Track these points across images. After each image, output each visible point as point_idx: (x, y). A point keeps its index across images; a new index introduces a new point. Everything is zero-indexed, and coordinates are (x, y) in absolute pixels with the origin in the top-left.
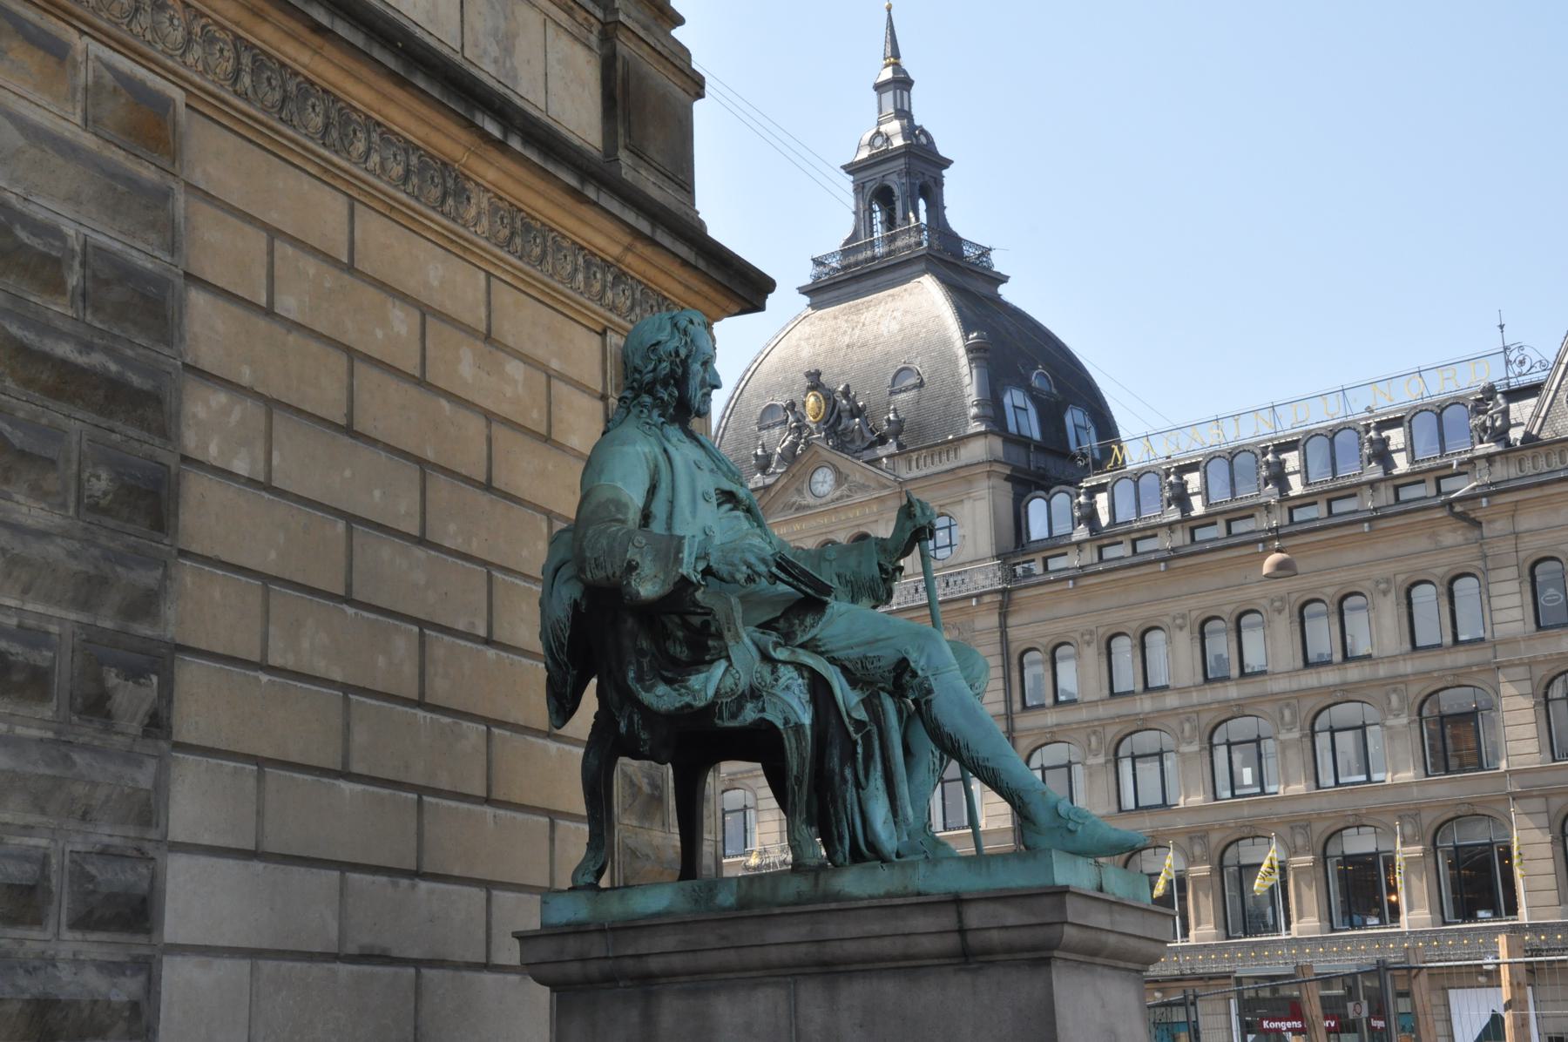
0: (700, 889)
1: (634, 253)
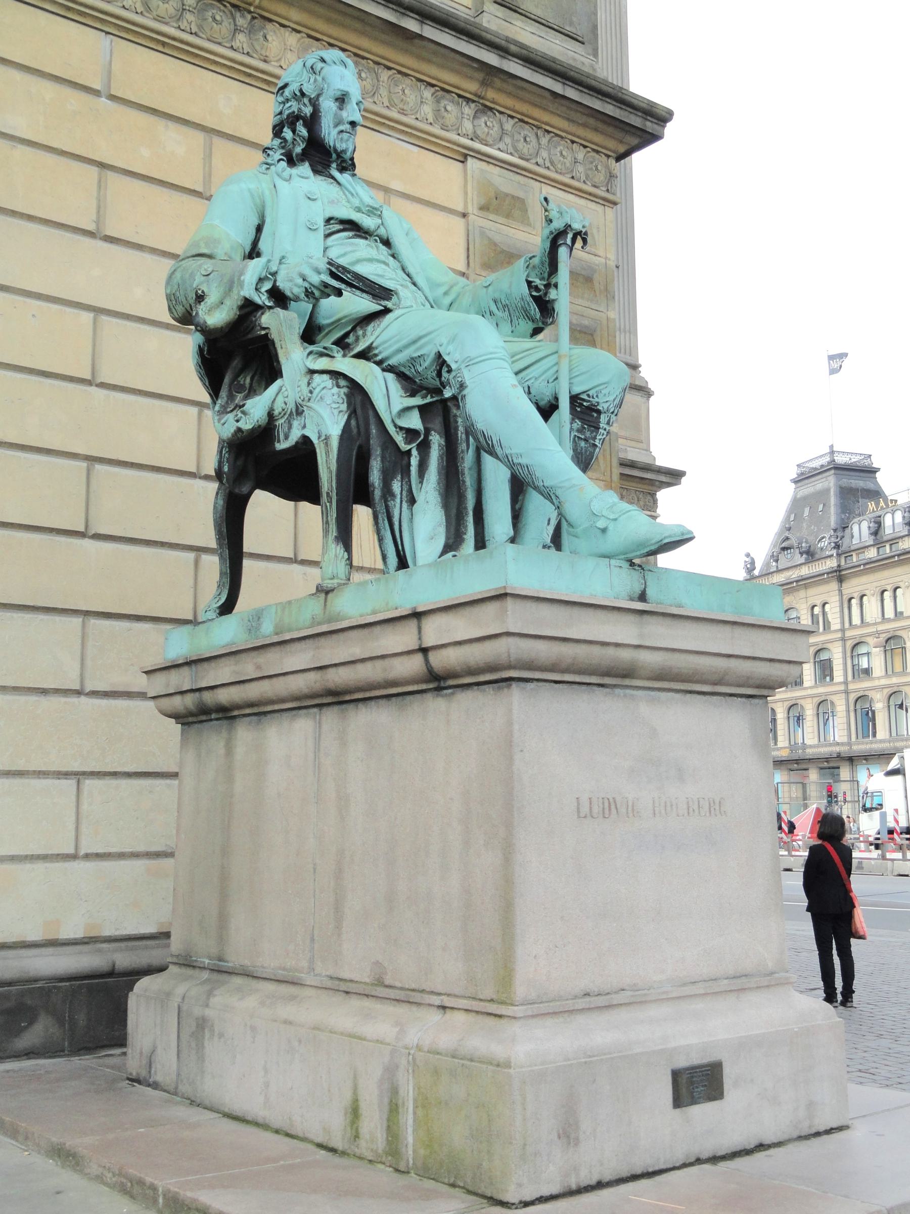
0: (253, 619)
1: (493, 87)
